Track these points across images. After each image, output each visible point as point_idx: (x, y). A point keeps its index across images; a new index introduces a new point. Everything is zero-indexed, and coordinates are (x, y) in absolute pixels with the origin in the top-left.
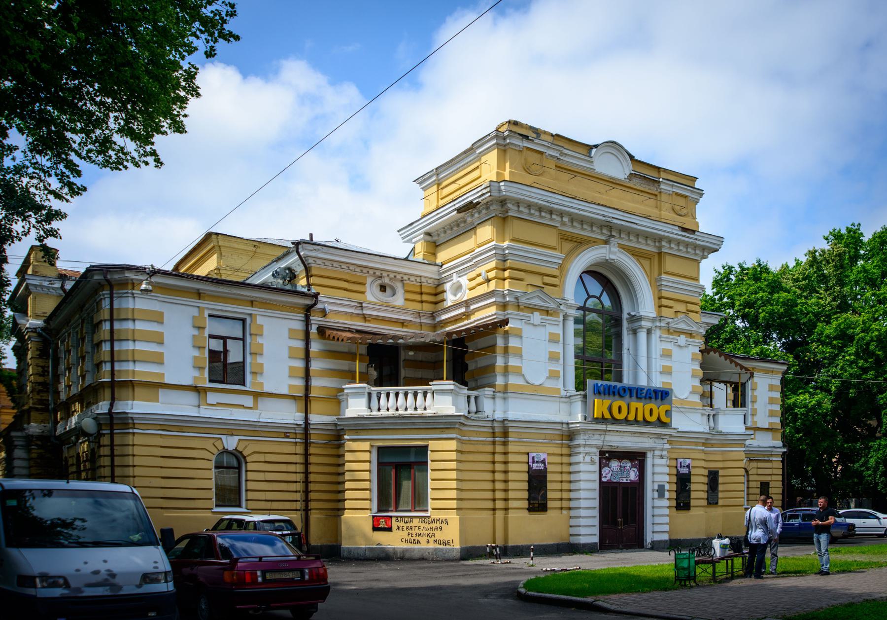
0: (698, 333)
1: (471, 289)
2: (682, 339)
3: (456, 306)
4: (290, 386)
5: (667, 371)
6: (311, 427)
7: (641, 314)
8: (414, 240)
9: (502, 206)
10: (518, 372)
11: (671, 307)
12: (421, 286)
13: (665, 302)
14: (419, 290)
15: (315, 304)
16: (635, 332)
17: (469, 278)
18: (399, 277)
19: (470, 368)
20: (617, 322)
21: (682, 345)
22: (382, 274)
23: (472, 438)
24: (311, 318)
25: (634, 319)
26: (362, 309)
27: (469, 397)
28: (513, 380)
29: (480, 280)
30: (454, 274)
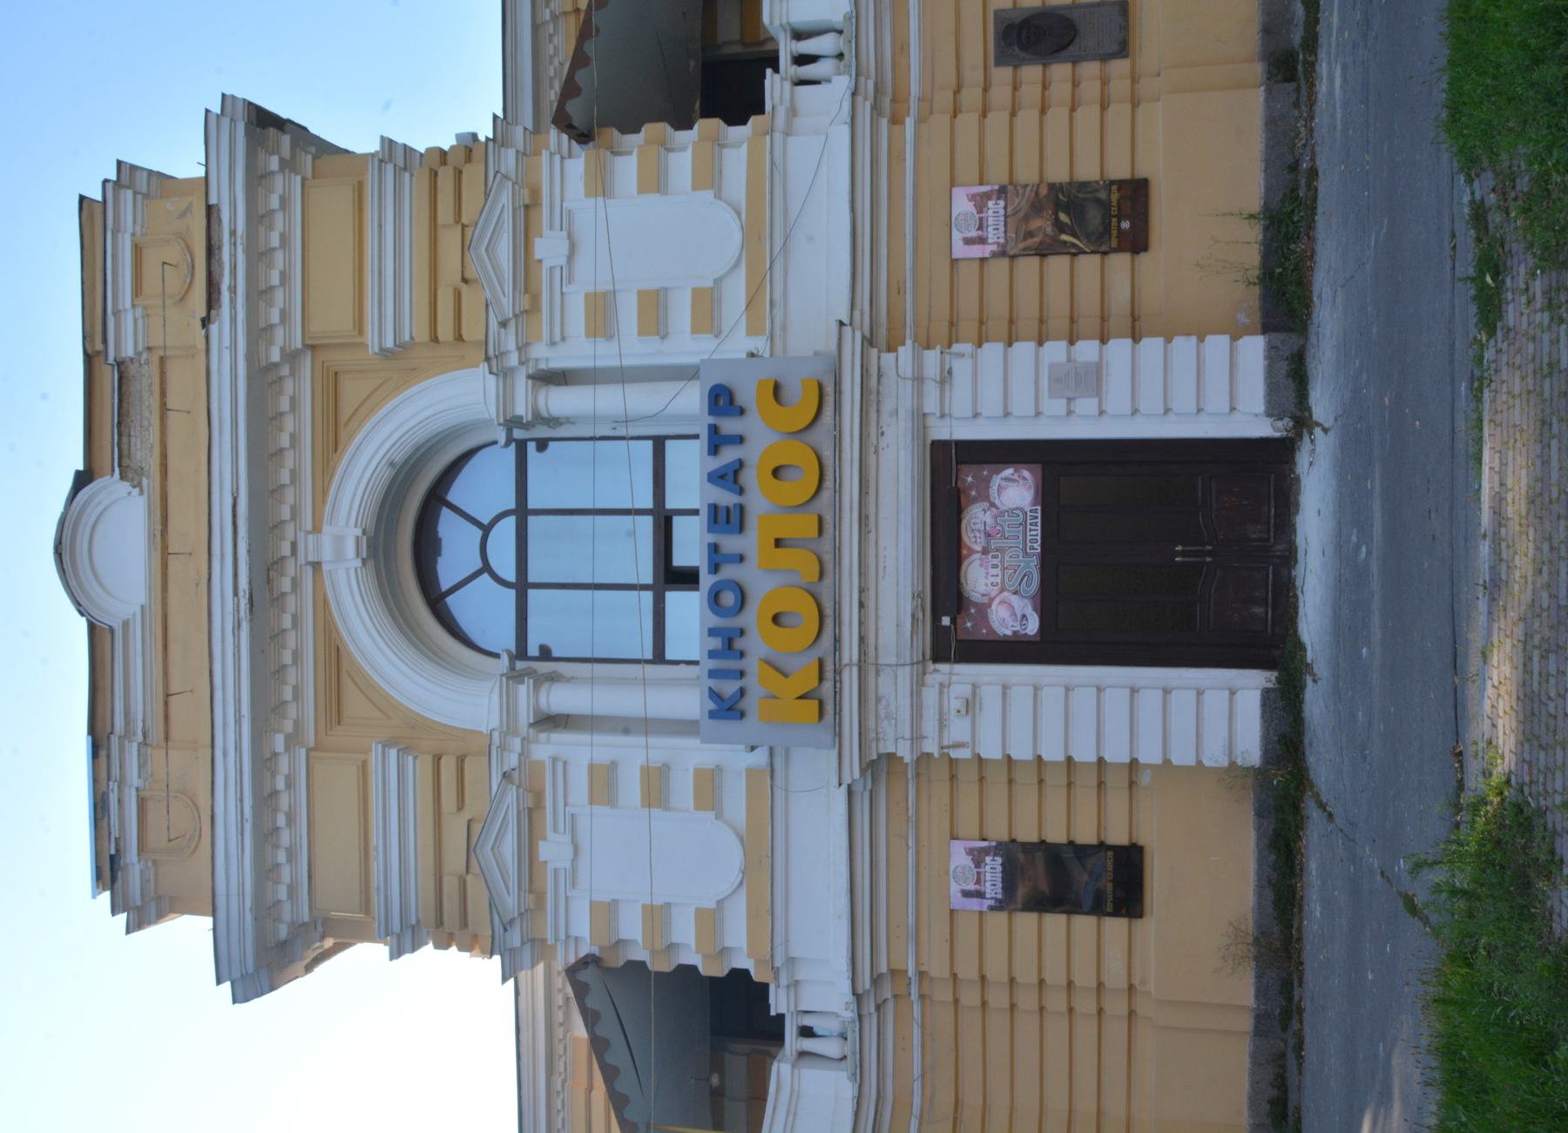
11: (458, 295)
13: (445, 331)
23: (917, 1070)
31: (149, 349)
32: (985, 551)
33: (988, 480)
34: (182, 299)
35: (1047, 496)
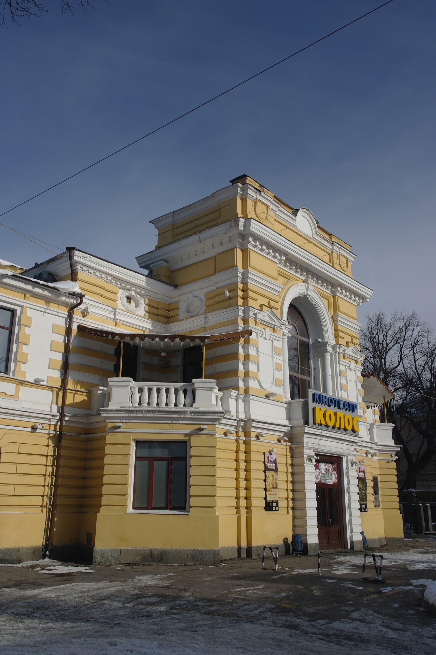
7: (326, 341)
15: (81, 303)
24: (74, 316)
26: (115, 315)
28: (253, 384)
32: (326, 469)
33: (335, 471)
35: (334, 484)
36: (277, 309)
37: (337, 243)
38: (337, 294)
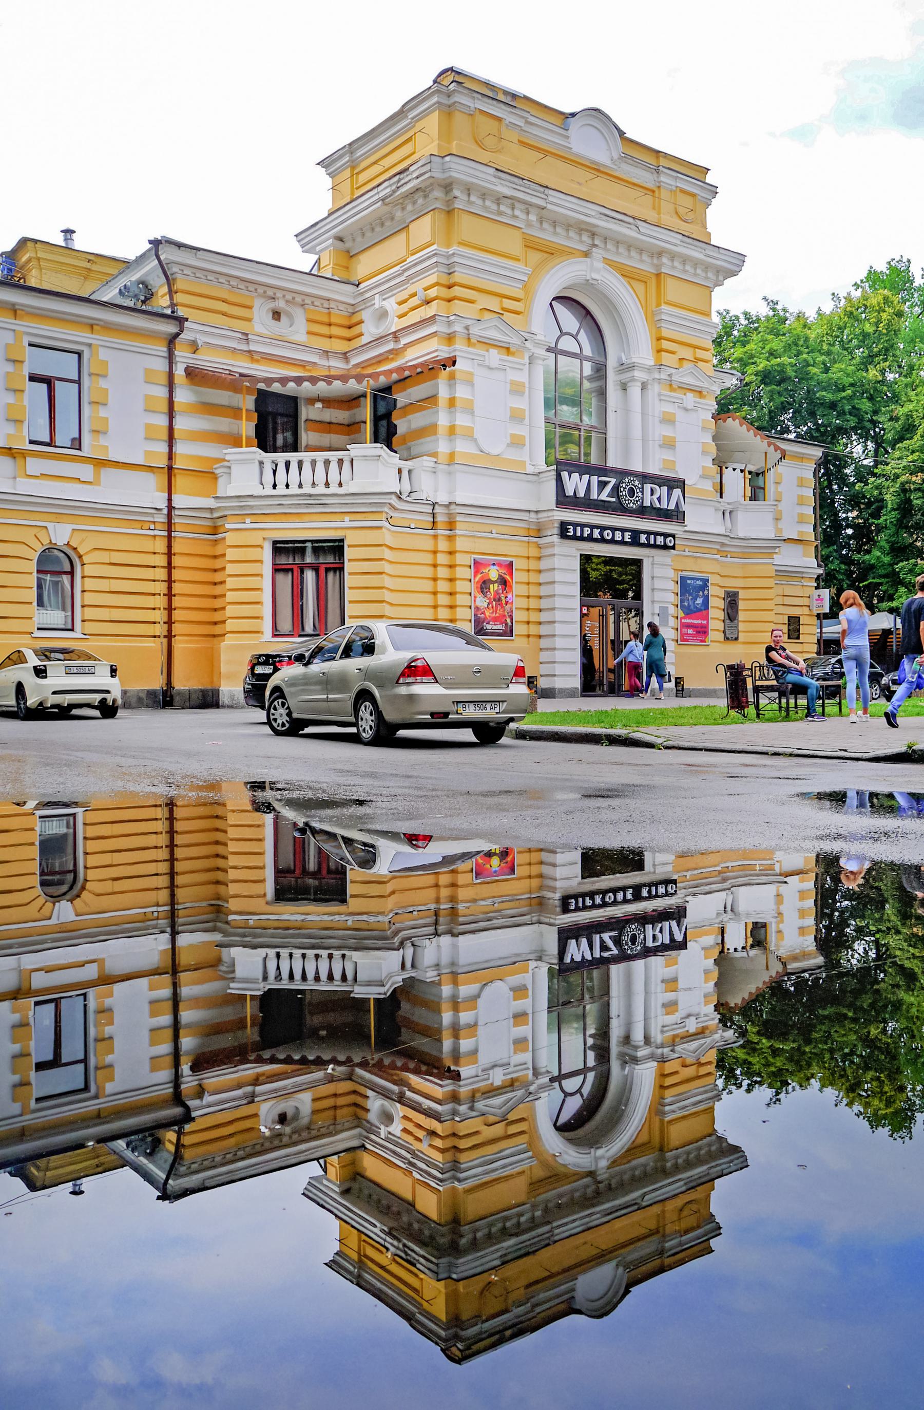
0: (710, 391)
1: (400, 317)
2: (690, 399)
3: (380, 340)
4: (147, 453)
5: (669, 444)
6: (177, 512)
7: (634, 360)
8: (318, 248)
9: (447, 193)
10: (469, 435)
12: (329, 313)
14: (326, 320)
16: (624, 387)
17: (399, 300)
18: (299, 299)
19: (399, 431)
20: (600, 371)
21: (689, 407)
22: (275, 294)
24: (176, 353)
25: (625, 368)
27: (400, 471)
28: (462, 447)
29: (415, 301)
30: (377, 296)
31: (659, 187)
34: (677, 213)
36: (518, 313)
37: (669, 169)
38: (663, 270)
